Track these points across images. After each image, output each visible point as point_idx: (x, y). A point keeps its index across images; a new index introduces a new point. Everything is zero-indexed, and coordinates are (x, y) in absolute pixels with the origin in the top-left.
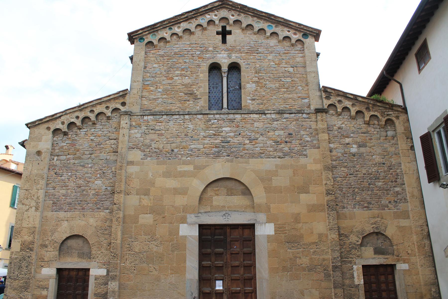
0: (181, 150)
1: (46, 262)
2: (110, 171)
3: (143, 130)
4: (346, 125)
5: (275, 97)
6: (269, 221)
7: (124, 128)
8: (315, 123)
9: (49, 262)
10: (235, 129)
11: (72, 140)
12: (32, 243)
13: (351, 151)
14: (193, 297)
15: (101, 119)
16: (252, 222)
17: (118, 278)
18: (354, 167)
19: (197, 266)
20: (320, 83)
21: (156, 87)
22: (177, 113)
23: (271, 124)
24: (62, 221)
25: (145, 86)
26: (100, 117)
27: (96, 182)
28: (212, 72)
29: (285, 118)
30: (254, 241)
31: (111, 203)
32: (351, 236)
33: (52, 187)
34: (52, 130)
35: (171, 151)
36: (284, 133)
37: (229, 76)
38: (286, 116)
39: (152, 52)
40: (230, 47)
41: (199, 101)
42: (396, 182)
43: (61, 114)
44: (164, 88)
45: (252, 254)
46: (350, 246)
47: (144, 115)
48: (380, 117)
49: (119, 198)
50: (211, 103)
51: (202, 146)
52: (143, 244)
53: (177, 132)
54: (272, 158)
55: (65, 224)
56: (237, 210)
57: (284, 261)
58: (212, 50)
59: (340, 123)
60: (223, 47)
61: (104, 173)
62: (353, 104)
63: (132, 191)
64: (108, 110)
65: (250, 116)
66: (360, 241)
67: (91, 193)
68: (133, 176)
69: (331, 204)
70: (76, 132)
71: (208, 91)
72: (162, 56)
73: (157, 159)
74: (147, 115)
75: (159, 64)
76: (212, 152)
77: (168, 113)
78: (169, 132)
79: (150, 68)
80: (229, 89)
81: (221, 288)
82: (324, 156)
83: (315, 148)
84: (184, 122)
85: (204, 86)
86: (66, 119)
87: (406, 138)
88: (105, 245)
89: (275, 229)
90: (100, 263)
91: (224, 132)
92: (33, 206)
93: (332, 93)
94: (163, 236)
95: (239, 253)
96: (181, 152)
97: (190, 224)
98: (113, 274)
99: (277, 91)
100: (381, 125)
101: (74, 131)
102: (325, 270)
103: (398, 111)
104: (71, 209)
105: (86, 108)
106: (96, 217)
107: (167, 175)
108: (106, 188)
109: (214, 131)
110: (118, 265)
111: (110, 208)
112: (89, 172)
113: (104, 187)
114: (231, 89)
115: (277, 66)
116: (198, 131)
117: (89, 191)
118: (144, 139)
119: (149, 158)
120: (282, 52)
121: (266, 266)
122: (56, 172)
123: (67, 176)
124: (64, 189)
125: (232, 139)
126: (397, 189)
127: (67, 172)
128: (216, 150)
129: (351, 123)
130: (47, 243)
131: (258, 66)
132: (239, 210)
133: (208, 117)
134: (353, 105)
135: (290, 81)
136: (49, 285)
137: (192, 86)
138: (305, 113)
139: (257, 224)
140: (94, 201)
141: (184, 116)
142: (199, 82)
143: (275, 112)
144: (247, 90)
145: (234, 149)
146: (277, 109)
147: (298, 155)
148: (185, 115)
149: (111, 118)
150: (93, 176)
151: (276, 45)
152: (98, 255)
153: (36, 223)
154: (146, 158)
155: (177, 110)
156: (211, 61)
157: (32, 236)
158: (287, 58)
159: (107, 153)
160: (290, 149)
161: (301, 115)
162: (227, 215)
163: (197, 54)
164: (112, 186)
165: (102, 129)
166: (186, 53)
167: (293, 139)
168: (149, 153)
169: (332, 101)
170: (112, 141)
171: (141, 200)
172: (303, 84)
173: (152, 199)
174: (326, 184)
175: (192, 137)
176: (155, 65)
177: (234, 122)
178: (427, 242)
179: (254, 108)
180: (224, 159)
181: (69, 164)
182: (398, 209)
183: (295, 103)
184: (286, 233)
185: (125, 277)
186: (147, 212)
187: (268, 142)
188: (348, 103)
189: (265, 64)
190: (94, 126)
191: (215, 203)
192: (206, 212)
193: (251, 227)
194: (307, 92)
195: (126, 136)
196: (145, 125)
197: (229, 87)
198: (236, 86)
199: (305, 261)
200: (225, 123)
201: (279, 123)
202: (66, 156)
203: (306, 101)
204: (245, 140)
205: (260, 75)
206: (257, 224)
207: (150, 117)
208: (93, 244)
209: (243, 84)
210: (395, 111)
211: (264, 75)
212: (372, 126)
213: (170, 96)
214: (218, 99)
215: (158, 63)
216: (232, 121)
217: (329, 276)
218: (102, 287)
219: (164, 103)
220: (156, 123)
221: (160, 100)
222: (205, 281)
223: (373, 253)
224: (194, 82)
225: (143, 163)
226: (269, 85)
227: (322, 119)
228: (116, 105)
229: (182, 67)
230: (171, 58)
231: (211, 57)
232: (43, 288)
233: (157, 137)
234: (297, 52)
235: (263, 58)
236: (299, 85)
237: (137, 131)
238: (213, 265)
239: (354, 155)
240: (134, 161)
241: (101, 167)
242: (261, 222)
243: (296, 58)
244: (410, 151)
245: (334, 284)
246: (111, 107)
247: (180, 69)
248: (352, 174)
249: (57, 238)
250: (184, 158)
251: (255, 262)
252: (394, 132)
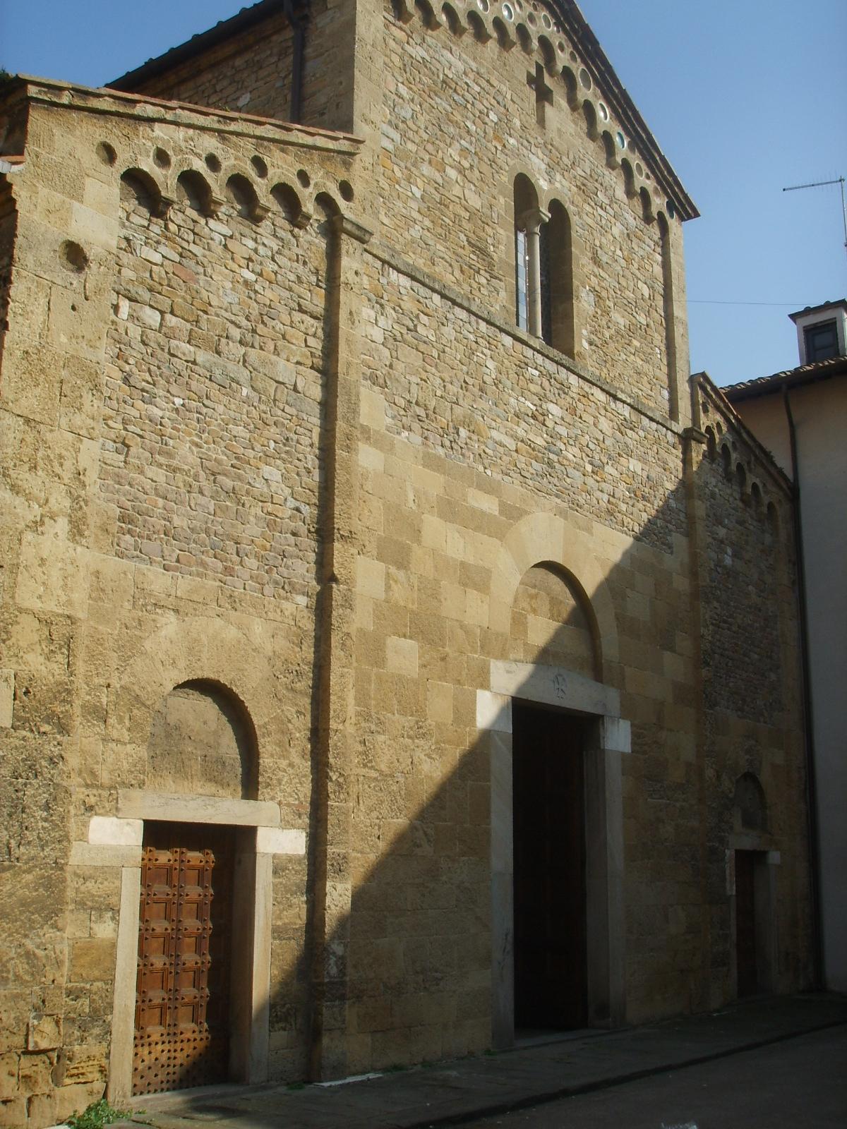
1: (102, 787)
12: (65, 692)
22: (465, 304)
47: (390, 265)
51: (511, 444)
55: (169, 625)
63: (367, 543)
74: (399, 271)
77: (447, 292)
106: (271, 615)
107: (451, 510)
108: (297, 504)
109: (535, 405)
119: (405, 434)
130: (104, 700)
219: (425, 246)
225: (392, 445)
228: (328, 184)
233: (420, 362)
237: (372, 313)
241: (280, 413)
249: (142, 684)
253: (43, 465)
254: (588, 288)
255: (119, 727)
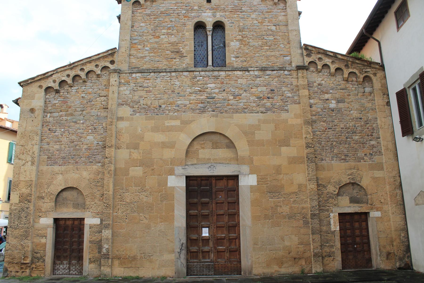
0: (168, 106)
1: (43, 212)
2: (101, 127)
3: (132, 87)
4: (325, 81)
5: (258, 55)
6: (251, 173)
7: (113, 85)
8: (296, 80)
9: (46, 212)
10: (219, 86)
11: (64, 97)
12: (30, 195)
13: (330, 107)
14: (182, 243)
15: (91, 76)
16: (235, 174)
17: (111, 227)
18: (333, 121)
19: (184, 214)
20: (302, 41)
21: (143, 45)
22: (164, 71)
23: (254, 80)
24: (57, 175)
25: (133, 45)
26: (90, 75)
27: (88, 137)
28: (197, 31)
29: (267, 75)
30: (238, 191)
31: (103, 157)
32: (329, 186)
33: (46, 142)
34: (44, 88)
35: (159, 107)
36: (266, 89)
37: (214, 35)
38: (268, 72)
39: (139, 11)
40: (215, 6)
41: (185, 59)
42: (372, 135)
43: (52, 73)
44: (151, 47)
45: (236, 203)
46: (328, 196)
47: (132, 73)
48: (358, 74)
49: (110, 152)
50: (197, 61)
51: (188, 102)
52: (134, 195)
53: (165, 88)
54: (255, 113)
55: (60, 177)
56: (222, 162)
57: (266, 209)
58: (197, 9)
59: (320, 79)
60: (208, 5)
61: (95, 128)
62: (332, 62)
63: (122, 146)
64: (98, 68)
65: (234, 73)
66: (337, 191)
67: (84, 147)
68: (123, 132)
69: (311, 156)
70: (67, 90)
71: (193, 49)
72: (149, 15)
73: (145, 115)
74: (136, 73)
75: (146, 23)
76: (198, 107)
77: (155, 71)
78: (156, 88)
79: (138, 27)
80: (214, 46)
81: (207, 235)
82: (305, 111)
83: (296, 104)
84: (171, 79)
85: (190, 44)
86: (57, 77)
87: (382, 94)
88: (98, 196)
89: (257, 180)
90: (93, 212)
91: (209, 88)
92: (29, 161)
93: (313, 50)
94: (153, 187)
95: (224, 202)
96: (168, 108)
97: (177, 176)
98: (106, 223)
99: (260, 48)
100: (359, 82)
101: (65, 89)
102: (304, 217)
103: (375, 68)
104: (65, 163)
105: (76, 66)
107: (155, 129)
108: (97, 142)
109: (200, 88)
110: (111, 215)
111: (101, 162)
112: (81, 127)
113: (96, 142)
114: (216, 47)
115: (260, 24)
116: (185, 88)
117: (82, 146)
118: (133, 96)
119: (137, 114)
120: (265, 11)
121: (250, 214)
122: (50, 129)
123: (60, 132)
124: (57, 145)
125: (217, 95)
126: (373, 143)
127: (60, 128)
128: (202, 105)
129: (330, 80)
130: (43, 195)
131: (242, 24)
132: (223, 162)
133: (193, 74)
134: (333, 62)
135: (273, 39)
136: (47, 233)
137: (178, 44)
138: (286, 70)
139: (241, 176)
140: (87, 155)
141: (171, 74)
142: (185, 40)
143: (258, 69)
144: (231, 48)
145: (219, 105)
146: (260, 66)
147: (280, 110)
148: (172, 73)
149: (100, 76)
150: (85, 131)
151: (260, 4)
152: (92, 206)
153: (32, 176)
154: (135, 114)
155: (164, 68)
156: (196, 20)
157: (29, 188)
158: (270, 16)
159: (98, 110)
160: (272, 105)
161: (282, 72)
162: (212, 167)
163: (182, 12)
164: (104, 141)
165: (93, 86)
166: (172, 12)
167: (275, 94)
168: (138, 109)
169: (313, 58)
170: (103, 98)
171: (131, 154)
172: (285, 42)
173: (141, 153)
174: (306, 138)
175: (179, 93)
176: (142, 24)
177: (219, 78)
178: (399, 192)
179: (238, 65)
180: (210, 114)
181: (62, 120)
182: (373, 161)
183: (277, 60)
184: (268, 183)
185: (118, 225)
186: (137, 165)
187: (251, 98)
188: (327, 61)
189: (248, 23)
190: (85, 84)
191: (201, 156)
192: (192, 165)
193: (235, 178)
194: (289, 50)
195: (115, 93)
196: (133, 82)
197: (214, 45)
198: (220, 44)
199: (285, 209)
200: (210, 80)
201: (261, 80)
202: (59, 113)
203: (288, 58)
204: (229, 96)
205: (244, 33)
206: (241, 176)
207: (138, 75)
208: (86, 195)
209: (227, 42)
210: (373, 68)
211: (247, 33)
212: (351, 82)
213: (157, 54)
214: (203, 57)
215: (145, 22)
216: (217, 77)
217: (308, 223)
218: (96, 235)
220: (144, 80)
221: (147, 58)
222: (192, 229)
223: (349, 202)
224: (180, 40)
226: (252, 43)
227: (303, 75)
228: (106, 64)
229: (168, 26)
230: (157, 17)
231: (197, 16)
232: (41, 236)
233: (145, 93)
234: (279, 11)
235: (247, 17)
236: (281, 43)
237: (126, 88)
238: (199, 214)
239: (333, 110)
240: (123, 117)
242: (244, 173)
243: (278, 17)
244: (386, 106)
245: (312, 230)
246: (100, 65)
247: (166, 28)
248: (331, 129)
250: (171, 114)
251: (239, 210)
252: (372, 88)
253: (25, 153)
254: (235, 41)
255: (47, 200)
